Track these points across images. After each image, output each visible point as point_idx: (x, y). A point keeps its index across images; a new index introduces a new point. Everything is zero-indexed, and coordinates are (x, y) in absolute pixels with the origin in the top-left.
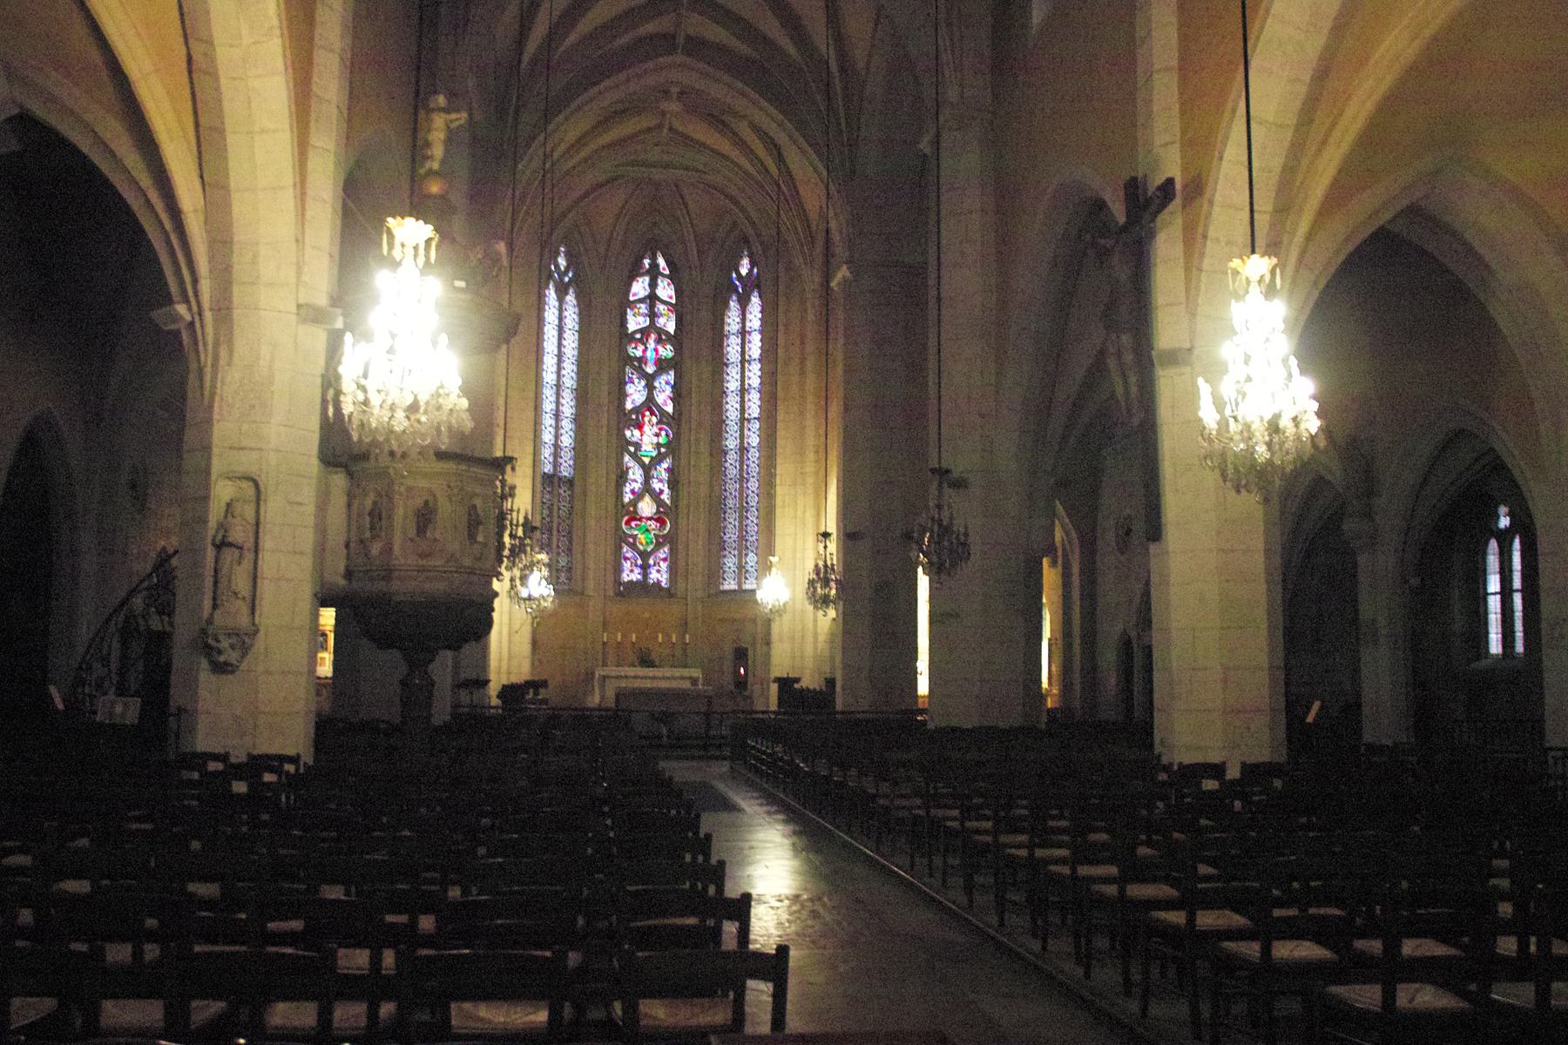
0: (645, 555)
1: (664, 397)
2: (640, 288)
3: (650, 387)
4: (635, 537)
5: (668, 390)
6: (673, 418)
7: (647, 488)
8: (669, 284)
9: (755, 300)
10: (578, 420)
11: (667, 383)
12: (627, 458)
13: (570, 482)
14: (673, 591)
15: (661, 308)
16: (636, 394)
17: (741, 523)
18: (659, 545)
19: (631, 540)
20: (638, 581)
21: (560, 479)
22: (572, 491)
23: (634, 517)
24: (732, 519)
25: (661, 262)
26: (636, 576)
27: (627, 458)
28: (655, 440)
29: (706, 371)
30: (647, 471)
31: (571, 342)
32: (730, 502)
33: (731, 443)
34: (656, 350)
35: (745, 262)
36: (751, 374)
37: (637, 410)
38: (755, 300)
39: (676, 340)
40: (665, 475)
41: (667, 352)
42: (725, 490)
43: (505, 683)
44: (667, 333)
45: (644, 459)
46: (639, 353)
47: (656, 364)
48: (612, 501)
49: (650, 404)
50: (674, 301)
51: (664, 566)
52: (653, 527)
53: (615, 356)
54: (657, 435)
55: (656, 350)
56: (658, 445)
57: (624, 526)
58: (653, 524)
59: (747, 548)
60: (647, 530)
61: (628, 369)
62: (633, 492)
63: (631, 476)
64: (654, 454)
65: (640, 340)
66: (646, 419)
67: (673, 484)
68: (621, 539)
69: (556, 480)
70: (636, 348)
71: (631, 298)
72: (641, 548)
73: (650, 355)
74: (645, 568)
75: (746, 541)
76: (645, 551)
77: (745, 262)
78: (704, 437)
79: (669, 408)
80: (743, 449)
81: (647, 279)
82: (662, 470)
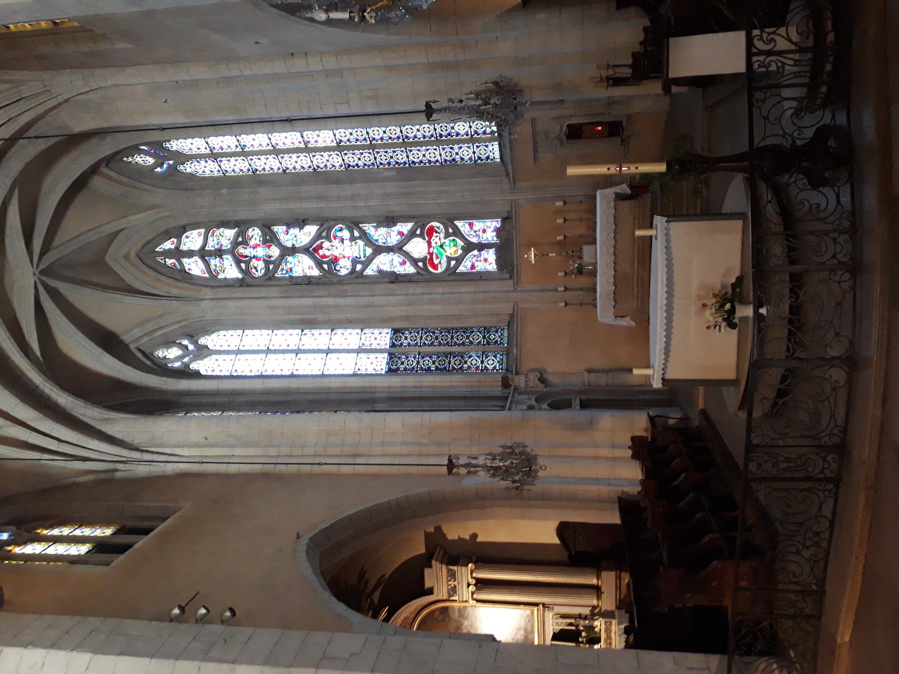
0: (469, 247)
1: (305, 235)
2: (195, 267)
3: (293, 251)
4: (449, 259)
5: (292, 231)
6: (322, 225)
7: (398, 249)
8: (187, 237)
9: (176, 145)
10: (333, 325)
11: (287, 232)
12: (369, 272)
13: (396, 331)
14: (505, 215)
15: (211, 245)
16: (303, 266)
17: (421, 144)
18: (457, 233)
19: (453, 263)
20: (497, 253)
21: (393, 345)
22: (407, 329)
23: (429, 260)
24: (417, 155)
25: (168, 245)
26: (491, 255)
27: (369, 272)
28: (347, 242)
29: (264, 192)
30: (379, 250)
31: (256, 338)
32: (402, 157)
33: (335, 161)
34: (255, 247)
35: (139, 159)
36: (256, 144)
37: (319, 264)
38: (176, 145)
39: (242, 226)
40: (383, 230)
41: (255, 234)
42: (389, 163)
43: (630, 453)
44: (237, 235)
45: (367, 255)
46: (261, 265)
47: (269, 247)
48: (412, 289)
49: (311, 250)
50: (203, 231)
51: (478, 225)
52: (437, 240)
53: (264, 292)
54: (342, 240)
55: (255, 247)
56: (353, 239)
57: (440, 270)
58: (435, 240)
59: (449, 134)
60: (441, 246)
61: (279, 274)
62: (404, 263)
63: (386, 268)
64: (361, 243)
65: (247, 263)
66: (327, 253)
67: (389, 221)
68: (452, 274)
69: (393, 350)
70: (256, 268)
71: (207, 275)
72: (460, 252)
73: (261, 252)
74: (481, 247)
75: (441, 136)
76: (463, 248)
77: (139, 159)
78: (334, 190)
79: (311, 230)
80: (340, 148)
81: (185, 261)
82: (380, 234)
